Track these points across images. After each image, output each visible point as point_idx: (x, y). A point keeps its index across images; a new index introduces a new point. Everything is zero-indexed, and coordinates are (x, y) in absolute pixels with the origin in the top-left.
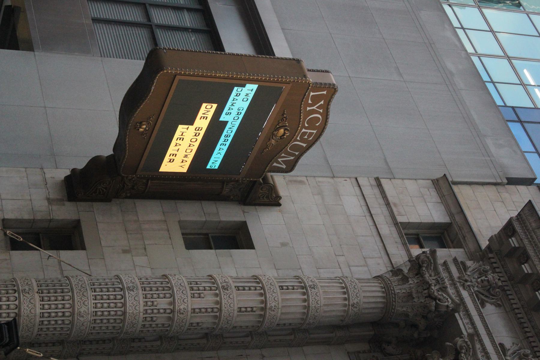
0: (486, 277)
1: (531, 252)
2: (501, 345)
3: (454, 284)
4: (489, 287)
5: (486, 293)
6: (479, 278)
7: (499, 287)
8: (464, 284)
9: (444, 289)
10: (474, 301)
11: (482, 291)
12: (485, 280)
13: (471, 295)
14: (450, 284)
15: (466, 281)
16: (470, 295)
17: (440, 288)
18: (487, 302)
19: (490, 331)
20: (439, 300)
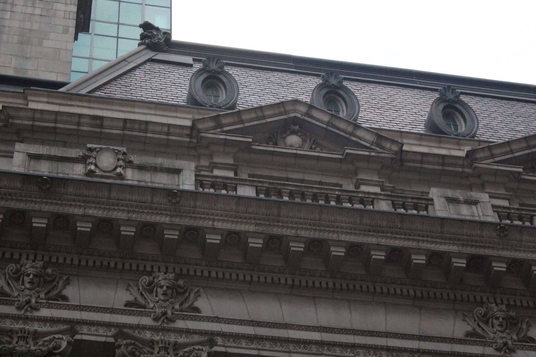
0: (28, 275)
1: (20, 206)
2: (128, 304)
3: (26, 319)
4: (42, 279)
5: (49, 287)
6: (23, 284)
7: (44, 268)
8: (31, 307)
9: (37, 336)
10: (61, 307)
11: (46, 291)
12: (32, 279)
13: (49, 306)
14: (25, 323)
15: (28, 302)
16: (48, 307)
17: (34, 339)
18: (61, 291)
19: (108, 309)
20: (54, 348)
